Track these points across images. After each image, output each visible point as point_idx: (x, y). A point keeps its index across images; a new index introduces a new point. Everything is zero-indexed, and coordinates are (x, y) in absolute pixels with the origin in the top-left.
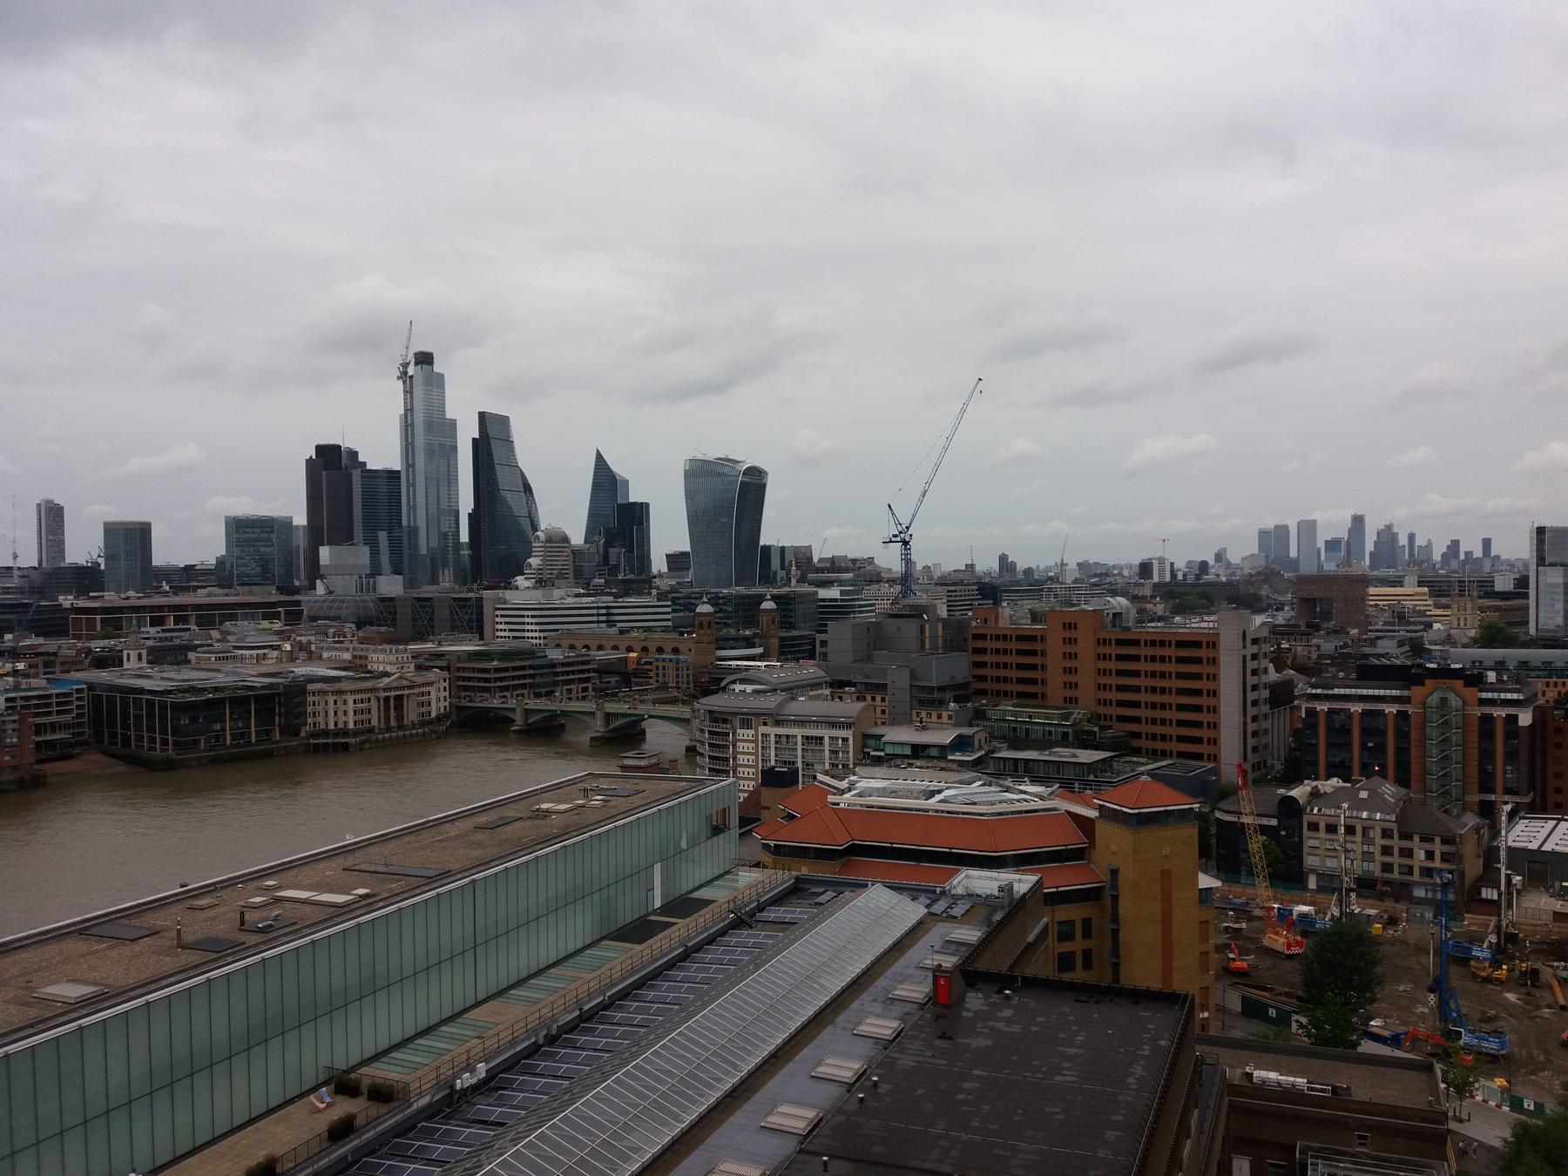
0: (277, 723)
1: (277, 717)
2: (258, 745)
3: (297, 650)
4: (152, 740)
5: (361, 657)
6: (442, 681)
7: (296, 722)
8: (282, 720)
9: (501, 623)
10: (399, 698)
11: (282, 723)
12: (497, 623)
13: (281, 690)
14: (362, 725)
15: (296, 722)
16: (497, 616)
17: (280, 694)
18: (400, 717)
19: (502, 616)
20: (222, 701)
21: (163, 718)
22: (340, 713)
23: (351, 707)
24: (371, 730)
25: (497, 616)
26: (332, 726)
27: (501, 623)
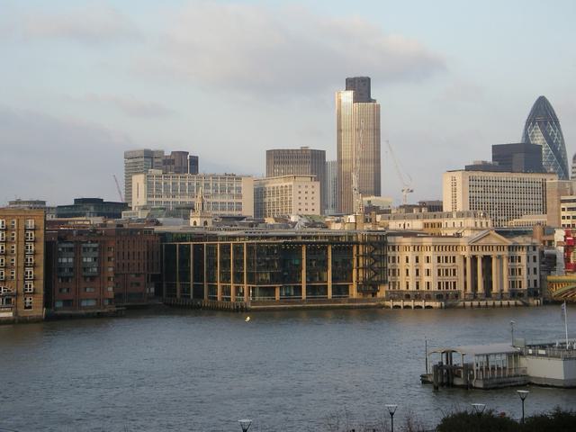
2: (335, 302)
3: (361, 221)
5: (433, 225)
6: (531, 249)
8: (361, 275)
9: (568, 218)
10: (487, 260)
12: (564, 218)
14: (447, 288)
16: (564, 209)
18: (488, 284)
19: (569, 209)
21: (239, 263)
22: (423, 273)
23: (433, 266)
24: (457, 296)
25: (564, 209)
26: (412, 287)
27: (568, 218)
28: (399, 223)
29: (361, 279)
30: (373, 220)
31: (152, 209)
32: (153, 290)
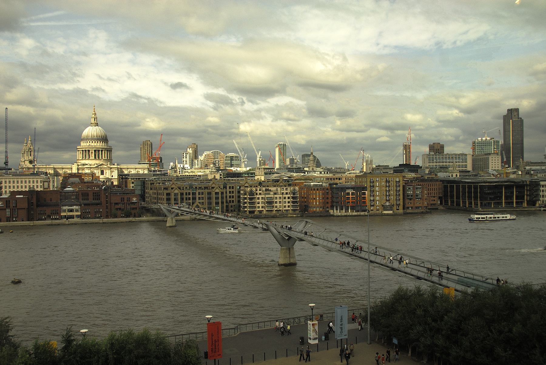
0: (525, 199)
1: (526, 196)
4: (470, 203)
7: (535, 199)
8: (528, 197)
11: (528, 199)
13: (528, 183)
15: (535, 199)
17: (527, 185)
20: (502, 186)
21: (476, 193)
28: (542, 175)
29: (528, 199)
30: (530, 173)
31: (431, 168)
32: (439, 202)
